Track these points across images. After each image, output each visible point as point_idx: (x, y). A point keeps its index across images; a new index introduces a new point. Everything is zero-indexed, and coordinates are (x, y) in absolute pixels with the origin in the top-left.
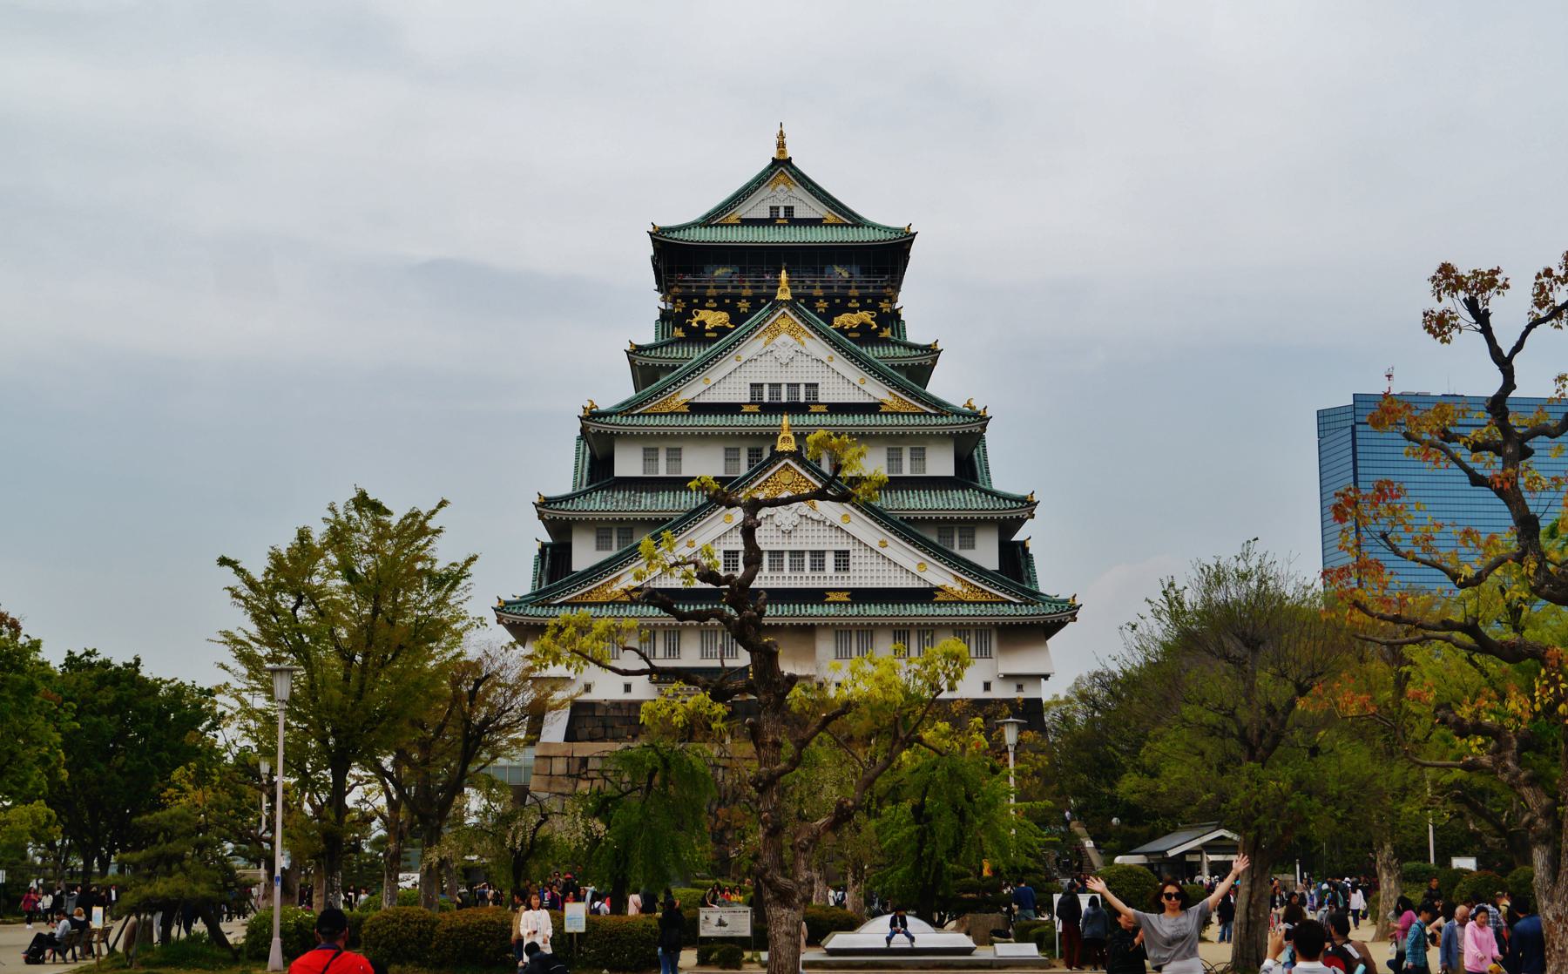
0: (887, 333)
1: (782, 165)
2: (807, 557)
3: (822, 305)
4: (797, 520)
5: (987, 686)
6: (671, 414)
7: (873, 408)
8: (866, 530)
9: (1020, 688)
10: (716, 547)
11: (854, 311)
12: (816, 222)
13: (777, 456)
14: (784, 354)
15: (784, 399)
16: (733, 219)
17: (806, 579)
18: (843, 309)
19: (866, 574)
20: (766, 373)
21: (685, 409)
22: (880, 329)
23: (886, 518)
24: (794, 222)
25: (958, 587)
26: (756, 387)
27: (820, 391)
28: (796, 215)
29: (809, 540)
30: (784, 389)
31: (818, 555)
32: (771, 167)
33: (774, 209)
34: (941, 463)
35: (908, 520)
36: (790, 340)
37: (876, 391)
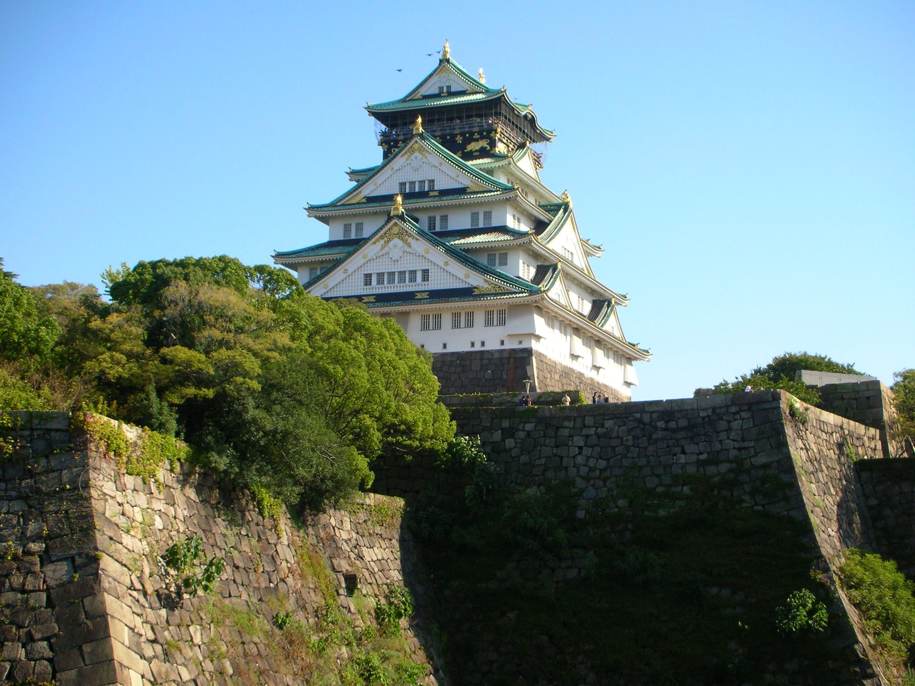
1: (444, 61)
2: (407, 274)
3: (459, 140)
4: (401, 254)
5: (502, 343)
6: (358, 203)
7: (462, 191)
8: (437, 255)
9: (520, 342)
11: (477, 140)
12: (463, 93)
13: (390, 218)
15: (417, 190)
16: (418, 96)
17: (407, 287)
18: (471, 140)
19: (438, 282)
21: (364, 201)
22: (491, 149)
24: (451, 94)
25: (486, 285)
26: (403, 185)
28: (453, 90)
29: (407, 265)
31: (413, 273)
32: (440, 64)
33: (441, 88)
35: (464, 250)
36: (420, 156)
37: (464, 181)
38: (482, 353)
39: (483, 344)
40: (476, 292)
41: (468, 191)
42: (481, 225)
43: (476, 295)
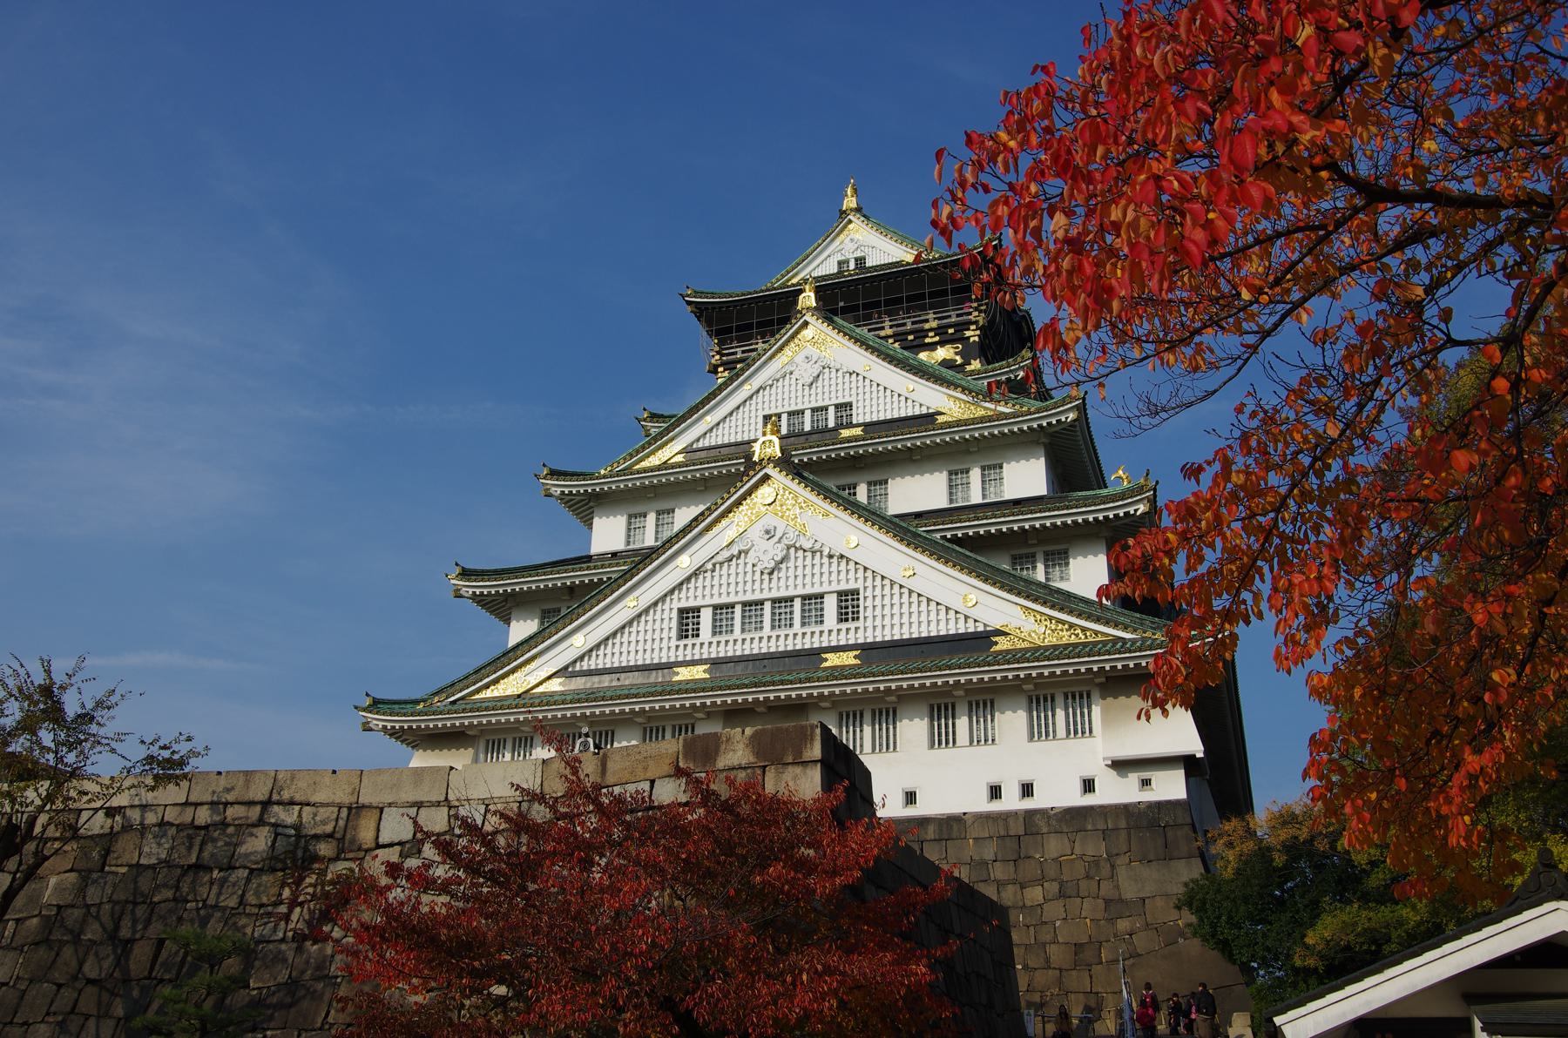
0: (976, 365)
5: (1088, 786)
7: (928, 419)
9: (1146, 783)
10: (667, 606)
11: (932, 347)
14: (806, 372)
15: (807, 428)
16: (794, 281)
17: (796, 637)
19: (885, 622)
20: (782, 400)
23: (916, 535)
27: (854, 412)
30: (808, 414)
31: (813, 600)
34: (1026, 477)
35: (955, 540)
38: (1030, 814)
39: (1027, 790)
40: (1003, 644)
41: (941, 419)
42: (976, 498)
43: (1001, 652)
